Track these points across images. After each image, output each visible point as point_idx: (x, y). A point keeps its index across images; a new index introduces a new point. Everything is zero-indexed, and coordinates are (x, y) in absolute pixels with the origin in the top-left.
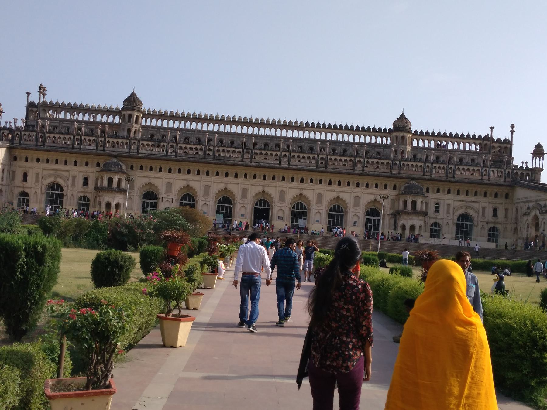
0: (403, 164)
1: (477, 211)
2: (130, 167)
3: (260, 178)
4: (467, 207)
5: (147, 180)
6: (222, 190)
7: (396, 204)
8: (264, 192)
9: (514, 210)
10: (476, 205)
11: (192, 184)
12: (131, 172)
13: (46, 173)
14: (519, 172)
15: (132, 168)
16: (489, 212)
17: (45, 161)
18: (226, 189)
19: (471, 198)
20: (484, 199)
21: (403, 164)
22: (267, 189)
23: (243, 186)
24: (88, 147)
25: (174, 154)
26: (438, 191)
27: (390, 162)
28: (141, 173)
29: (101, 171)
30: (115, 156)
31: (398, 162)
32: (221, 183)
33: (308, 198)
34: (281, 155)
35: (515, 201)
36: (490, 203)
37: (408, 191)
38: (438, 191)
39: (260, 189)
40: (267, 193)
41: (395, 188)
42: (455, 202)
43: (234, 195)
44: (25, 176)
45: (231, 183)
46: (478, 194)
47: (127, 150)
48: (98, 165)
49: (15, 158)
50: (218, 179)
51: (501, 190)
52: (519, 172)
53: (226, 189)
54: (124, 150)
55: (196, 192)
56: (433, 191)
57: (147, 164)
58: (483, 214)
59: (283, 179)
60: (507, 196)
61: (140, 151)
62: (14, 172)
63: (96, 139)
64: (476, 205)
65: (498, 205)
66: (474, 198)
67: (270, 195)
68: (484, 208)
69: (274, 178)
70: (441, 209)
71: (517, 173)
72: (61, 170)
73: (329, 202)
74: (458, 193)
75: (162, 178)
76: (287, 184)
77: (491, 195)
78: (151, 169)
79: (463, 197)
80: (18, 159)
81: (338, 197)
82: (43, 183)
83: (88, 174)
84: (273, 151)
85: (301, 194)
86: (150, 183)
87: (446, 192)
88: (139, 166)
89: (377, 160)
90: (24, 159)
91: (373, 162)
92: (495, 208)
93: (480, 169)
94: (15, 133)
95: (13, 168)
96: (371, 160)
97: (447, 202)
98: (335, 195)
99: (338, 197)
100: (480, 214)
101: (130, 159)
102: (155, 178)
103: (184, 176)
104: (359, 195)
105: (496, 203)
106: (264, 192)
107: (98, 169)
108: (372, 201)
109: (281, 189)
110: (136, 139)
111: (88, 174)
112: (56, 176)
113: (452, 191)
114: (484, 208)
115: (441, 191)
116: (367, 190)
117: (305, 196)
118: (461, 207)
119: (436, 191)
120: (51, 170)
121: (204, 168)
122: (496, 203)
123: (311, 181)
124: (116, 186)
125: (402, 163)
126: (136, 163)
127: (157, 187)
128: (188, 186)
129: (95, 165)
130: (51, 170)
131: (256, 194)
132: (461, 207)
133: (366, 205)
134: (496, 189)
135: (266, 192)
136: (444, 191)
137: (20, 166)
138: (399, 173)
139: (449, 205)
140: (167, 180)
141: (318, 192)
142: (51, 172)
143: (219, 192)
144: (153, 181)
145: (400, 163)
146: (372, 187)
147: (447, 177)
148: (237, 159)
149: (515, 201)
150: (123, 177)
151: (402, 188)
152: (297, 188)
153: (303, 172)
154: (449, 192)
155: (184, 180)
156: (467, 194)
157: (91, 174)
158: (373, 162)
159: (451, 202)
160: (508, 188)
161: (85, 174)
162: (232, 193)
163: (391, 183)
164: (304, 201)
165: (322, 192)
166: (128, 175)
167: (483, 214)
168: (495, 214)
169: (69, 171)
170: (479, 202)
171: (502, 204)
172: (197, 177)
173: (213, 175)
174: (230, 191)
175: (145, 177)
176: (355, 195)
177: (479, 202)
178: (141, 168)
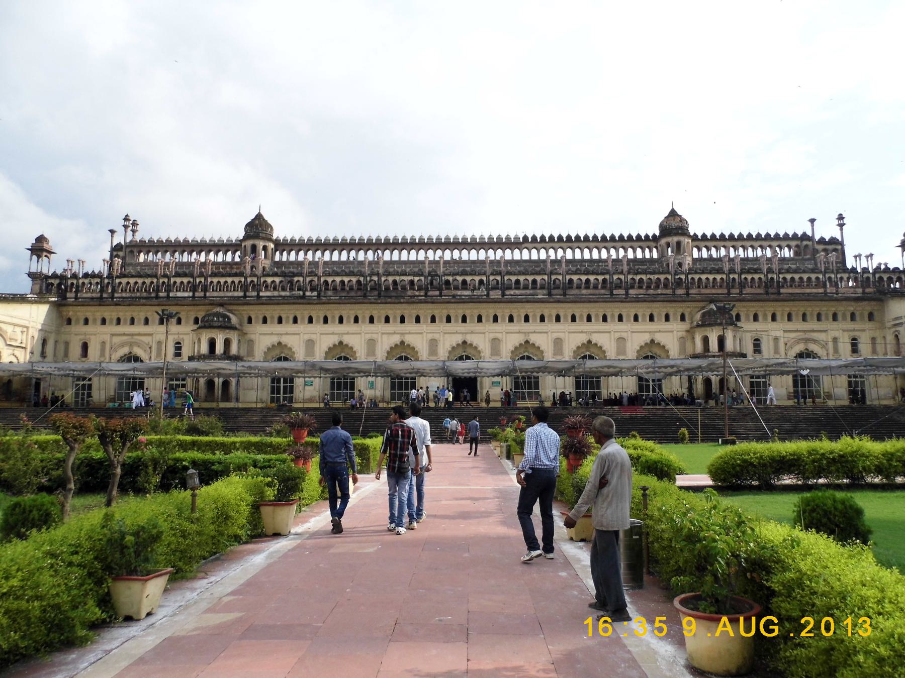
0: (693, 279)
1: (824, 346)
2: (246, 320)
3: (457, 321)
4: (807, 340)
5: (275, 340)
6: (396, 345)
7: (689, 345)
8: (464, 342)
9: (890, 338)
10: (821, 336)
11: (347, 340)
12: (248, 328)
13: (116, 340)
14: (885, 277)
15: (250, 321)
16: (845, 347)
17: (115, 322)
18: (402, 343)
19: (812, 325)
20: (835, 325)
21: (693, 279)
22: (470, 339)
23: (430, 336)
24: (179, 294)
25: (315, 293)
26: (756, 318)
27: (669, 277)
28: (265, 328)
29: (200, 328)
30: (221, 305)
31: (683, 277)
32: (395, 333)
33: (539, 348)
34: (488, 281)
35: (889, 325)
36: (844, 331)
37: (707, 321)
38: (756, 318)
39: (459, 339)
40: (471, 345)
41: (683, 318)
42: (787, 335)
43: (417, 352)
44: (85, 347)
45: (410, 333)
46: (823, 318)
47: (241, 294)
48: (196, 321)
49: (69, 322)
50: (389, 328)
51: (842, 309)
52: (885, 277)
53: (402, 343)
54: (236, 294)
55: (355, 352)
56: (747, 319)
57: (272, 311)
58: (836, 350)
59: (495, 319)
60: (871, 317)
61: (261, 294)
62: (67, 344)
63: (191, 280)
64: (821, 336)
65: (857, 334)
66: (815, 325)
67: (476, 348)
68: (835, 340)
69: (480, 319)
70: (764, 347)
71: (881, 278)
72: (139, 334)
73: (574, 352)
74: (790, 318)
75: (298, 334)
76: (503, 326)
77: (844, 318)
78: (280, 321)
79: (797, 325)
80: (73, 322)
81: (589, 342)
82: (113, 357)
83: (181, 336)
84: (475, 274)
85: (527, 342)
86: (280, 343)
87: (770, 318)
88: (261, 317)
89: (649, 276)
90: (82, 321)
91: (641, 280)
92: (854, 339)
93: (821, 276)
94: (70, 282)
95: (64, 338)
96: (638, 278)
97: (774, 334)
98: (583, 338)
99: (589, 342)
100: (831, 351)
101: (246, 307)
102: (287, 334)
103: (333, 327)
104: (624, 335)
105: (854, 330)
106: (464, 342)
107: (196, 327)
108: (646, 344)
109: (492, 336)
110: (255, 275)
111: (181, 336)
112: (131, 345)
113: (778, 317)
114: (835, 340)
115: (760, 318)
116: (637, 326)
117: (533, 344)
118: (798, 341)
119: (752, 318)
120: (124, 334)
121: (364, 311)
122: (854, 330)
123: (542, 319)
124: (222, 351)
125: (690, 277)
126: (256, 312)
127: (290, 349)
128: (341, 343)
129: (192, 321)
130: (124, 334)
131: (453, 348)
132: (798, 341)
133: (638, 351)
134: (851, 307)
135: (469, 342)
136: (765, 319)
137: (77, 334)
138: (688, 294)
139: (776, 339)
140: (307, 337)
141: (555, 335)
142: (125, 338)
143: (391, 348)
144: (285, 340)
145: (687, 277)
146: (644, 320)
147: (767, 293)
148: (417, 293)
149: (889, 325)
150: (234, 337)
151: (698, 316)
152: (519, 332)
153: (528, 305)
154: (774, 318)
155: (333, 334)
156: (790, 318)
157: (185, 337)
158: (641, 280)
159: (779, 334)
160: (873, 303)
161: (176, 337)
162: (413, 348)
163: (675, 310)
164: (532, 353)
165: (561, 335)
166: (243, 334)
167: (836, 350)
168: (855, 349)
169: (151, 335)
170: (825, 331)
171: (864, 330)
172: (354, 328)
173: (379, 321)
174: (409, 345)
175: (272, 334)
176: (617, 335)
177: (825, 331)
178: (265, 321)
